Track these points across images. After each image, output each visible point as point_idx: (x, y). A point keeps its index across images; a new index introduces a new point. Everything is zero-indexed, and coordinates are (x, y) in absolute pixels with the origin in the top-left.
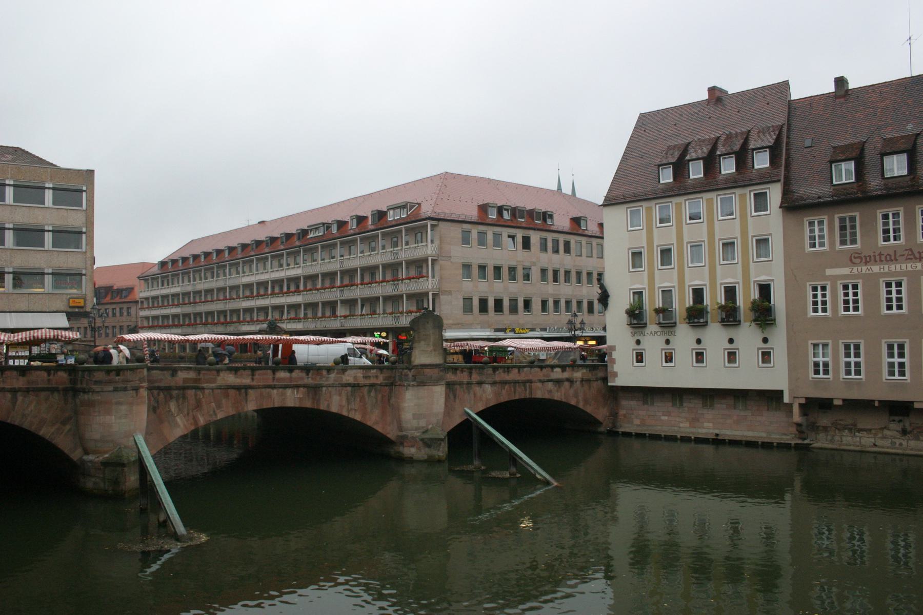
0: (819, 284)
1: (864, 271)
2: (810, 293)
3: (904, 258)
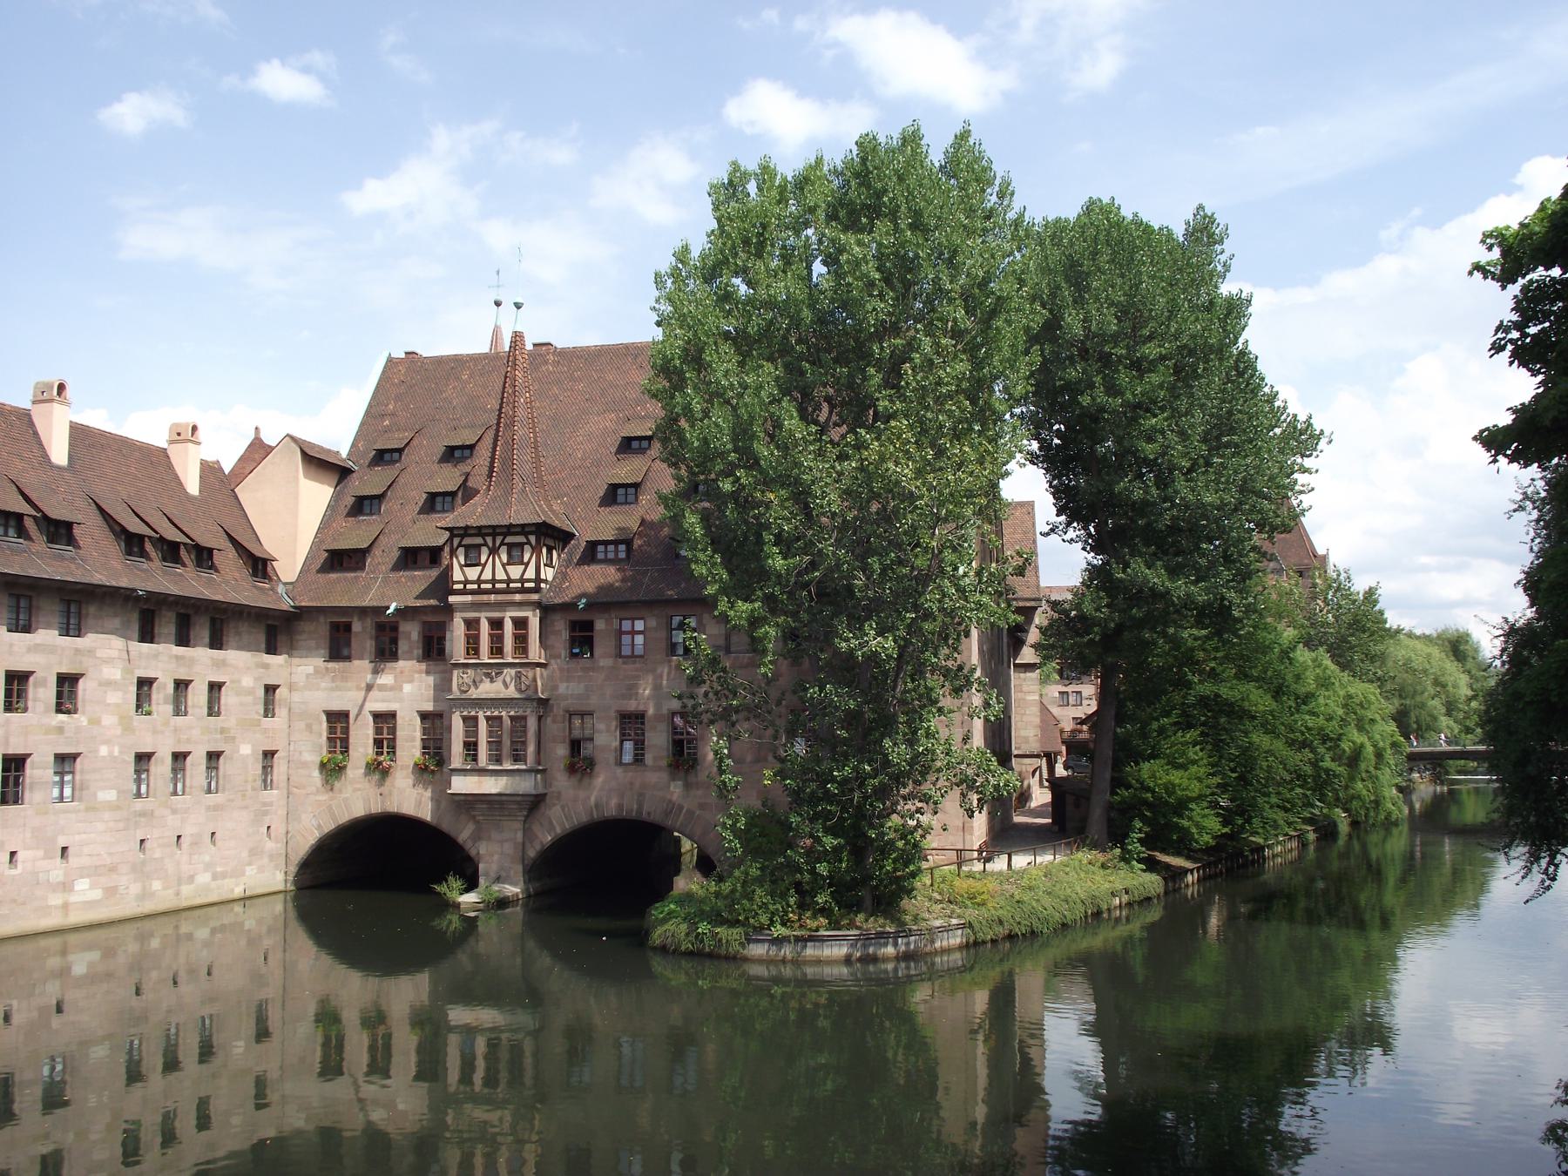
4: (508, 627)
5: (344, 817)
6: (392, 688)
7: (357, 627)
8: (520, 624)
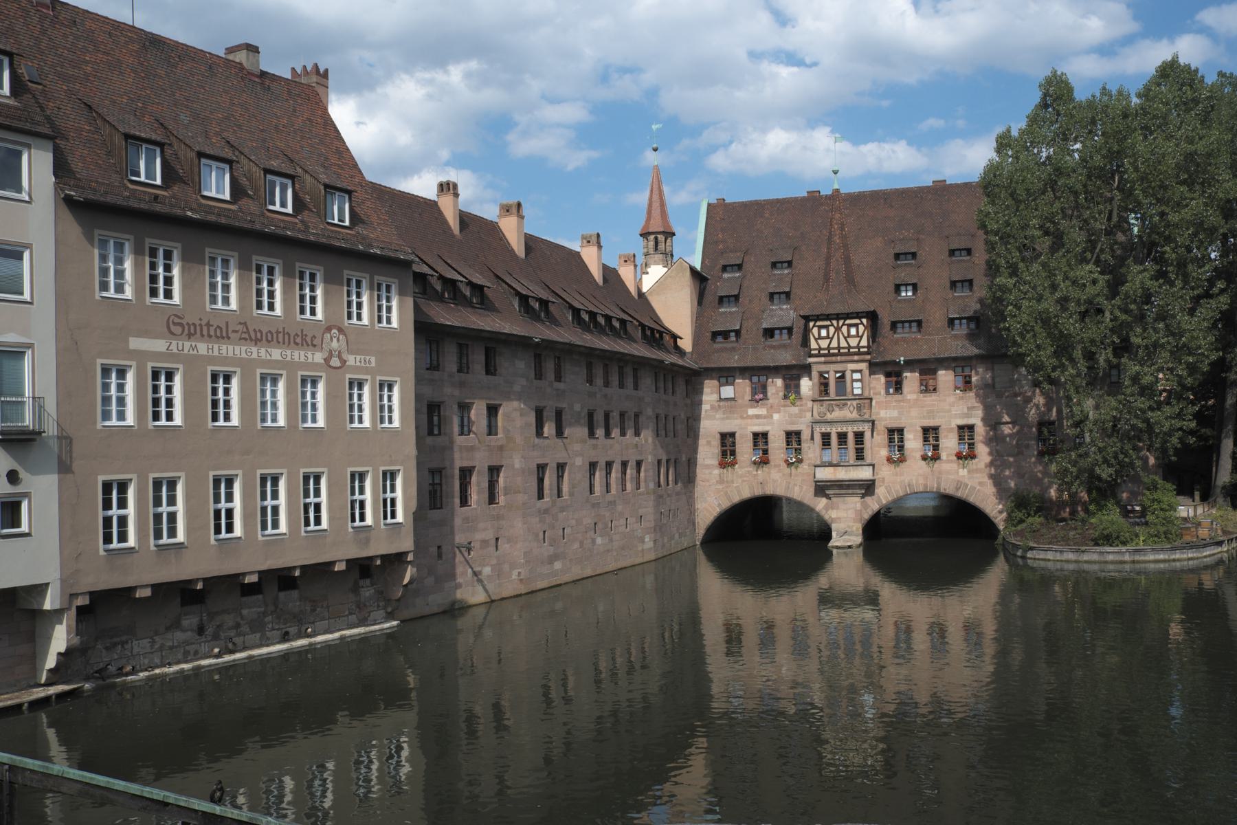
1: (186, 351)
3: (238, 335)
5: (736, 499)
6: (765, 417)
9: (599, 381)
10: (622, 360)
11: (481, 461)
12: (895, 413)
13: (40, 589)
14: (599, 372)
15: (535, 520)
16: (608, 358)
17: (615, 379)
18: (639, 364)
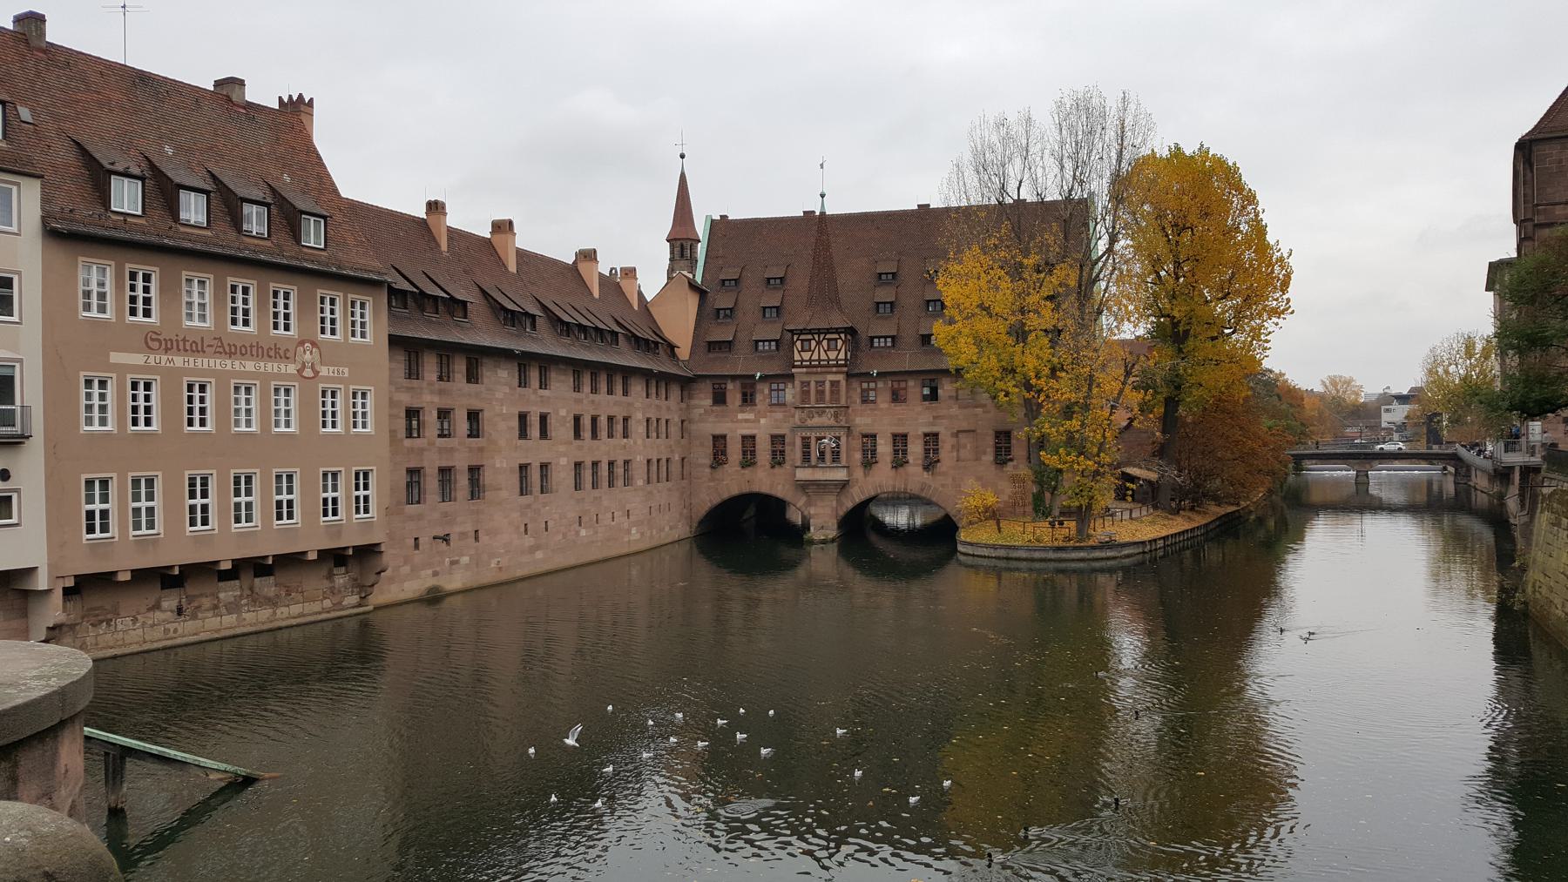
0: (97, 375)
2: (83, 391)
4: (828, 385)
5: (726, 496)
7: (730, 386)
8: (834, 384)
9: (587, 388)
10: (611, 370)
11: (461, 462)
12: (869, 421)
13: (30, 572)
14: (586, 379)
15: (515, 515)
16: (595, 368)
17: (603, 386)
18: (628, 373)
